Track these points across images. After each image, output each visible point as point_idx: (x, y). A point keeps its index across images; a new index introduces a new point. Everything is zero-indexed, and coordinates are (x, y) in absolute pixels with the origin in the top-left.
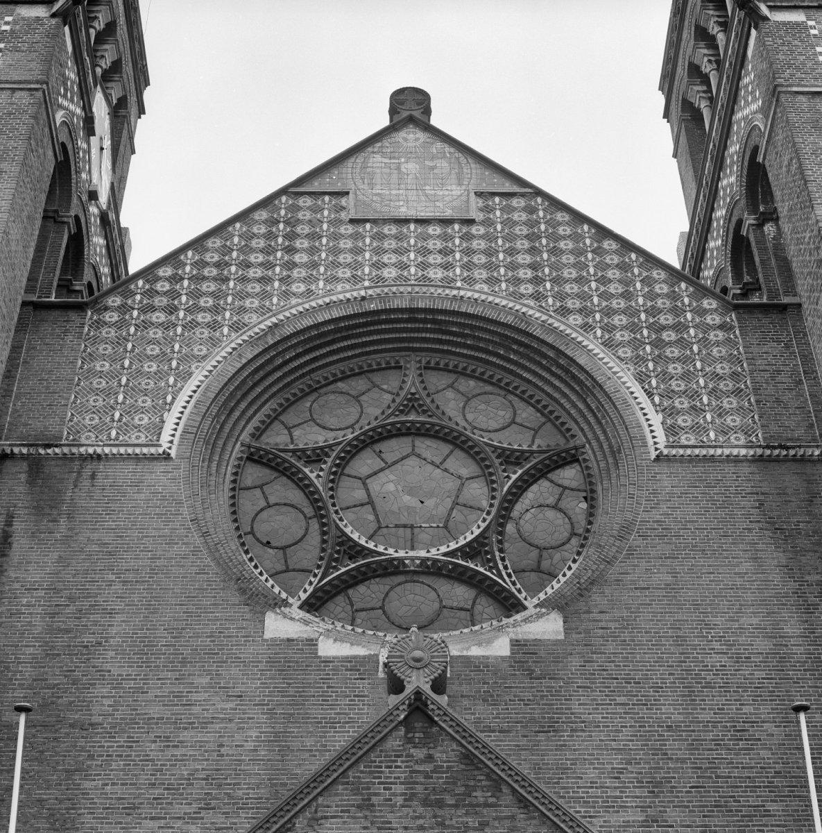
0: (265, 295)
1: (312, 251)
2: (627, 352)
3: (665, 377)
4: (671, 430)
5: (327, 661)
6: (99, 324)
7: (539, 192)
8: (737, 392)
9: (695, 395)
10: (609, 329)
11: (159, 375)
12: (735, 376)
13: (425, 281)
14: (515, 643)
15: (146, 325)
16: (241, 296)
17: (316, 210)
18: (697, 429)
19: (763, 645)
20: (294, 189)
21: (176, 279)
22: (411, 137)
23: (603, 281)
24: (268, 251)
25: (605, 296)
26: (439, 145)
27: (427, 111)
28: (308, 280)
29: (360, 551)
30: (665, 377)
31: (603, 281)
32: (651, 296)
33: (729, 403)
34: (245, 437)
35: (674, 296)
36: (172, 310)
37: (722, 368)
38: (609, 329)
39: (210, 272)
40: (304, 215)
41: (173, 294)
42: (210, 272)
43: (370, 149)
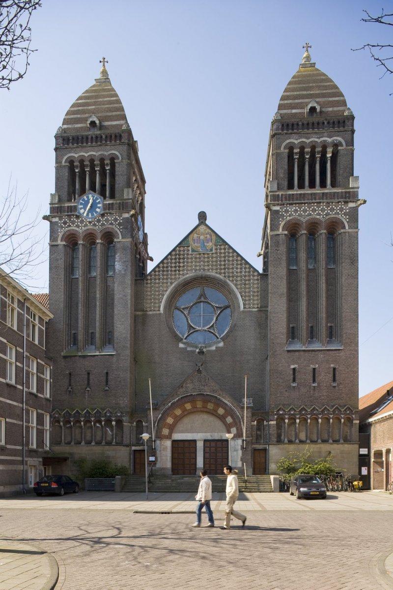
0: (175, 275)
1: (184, 262)
2: (239, 287)
3: (245, 292)
4: (244, 305)
5: (189, 351)
6: (147, 283)
7: (227, 244)
8: (257, 296)
9: (249, 296)
10: (237, 281)
11: (159, 295)
12: (258, 292)
13: (204, 270)
14: (216, 348)
15: (155, 283)
16: (171, 275)
17: (184, 251)
18: (249, 304)
19: (253, 347)
20: (179, 245)
21: (159, 271)
22: (202, 228)
23: (237, 268)
24: (175, 263)
25: (237, 272)
26: (208, 230)
27: (206, 220)
28: (183, 270)
29: (194, 328)
30: (245, 292)
31: (237, 268)
32: (245, 272)
33: (256, 298)
34: (174, 305)
35: (249, 272)
36: (159, 279)
37: (256, 290)
38: (237, 281)
39: (165, 269)
40: (182, 253)
41: (159, 275)
42: (165, 269)
43: (194, 232)
